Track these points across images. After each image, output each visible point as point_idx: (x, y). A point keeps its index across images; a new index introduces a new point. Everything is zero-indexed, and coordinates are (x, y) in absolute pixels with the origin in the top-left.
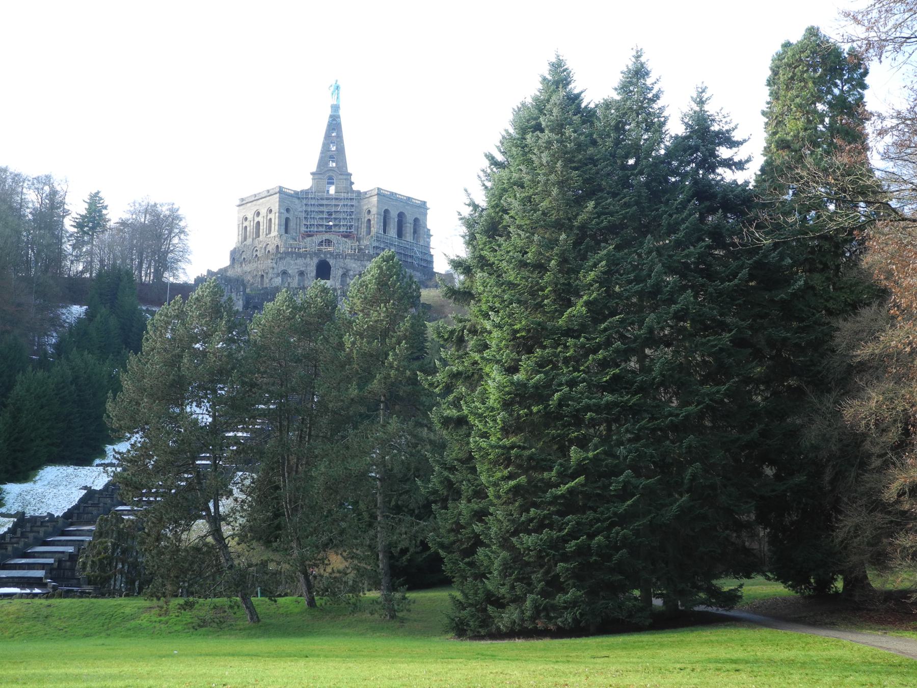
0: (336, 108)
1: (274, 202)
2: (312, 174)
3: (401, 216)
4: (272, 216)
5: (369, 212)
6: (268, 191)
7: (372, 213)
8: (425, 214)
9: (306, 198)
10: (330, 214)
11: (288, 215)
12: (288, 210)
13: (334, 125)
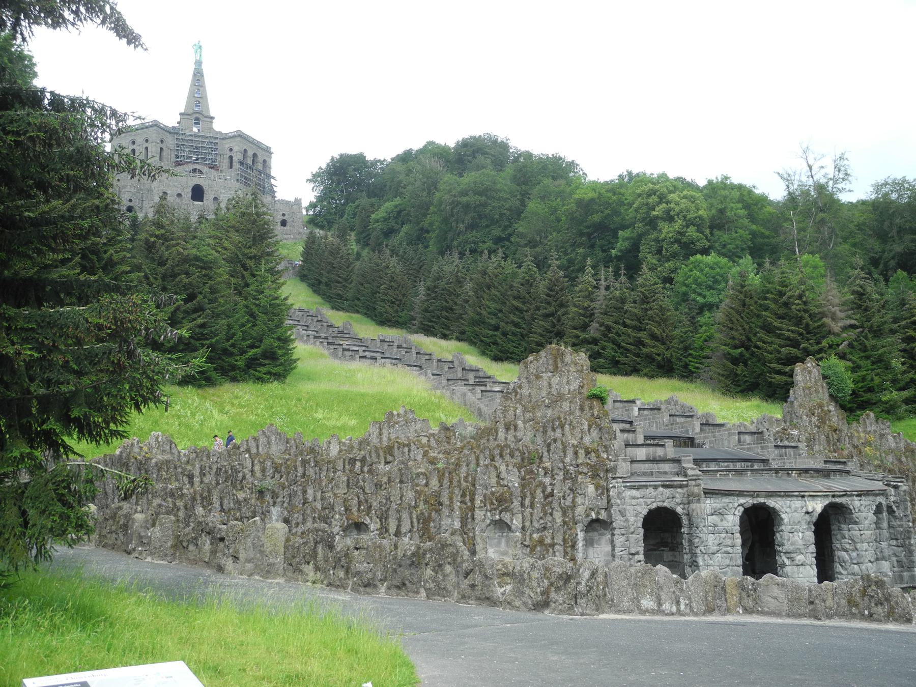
0: (199, 63)
2: (181, 114)
3: (255, 155)
5: (231, 150)
8: (270, 158)
10: (197, 148)
12: (162, 141)
13: (198, 77)
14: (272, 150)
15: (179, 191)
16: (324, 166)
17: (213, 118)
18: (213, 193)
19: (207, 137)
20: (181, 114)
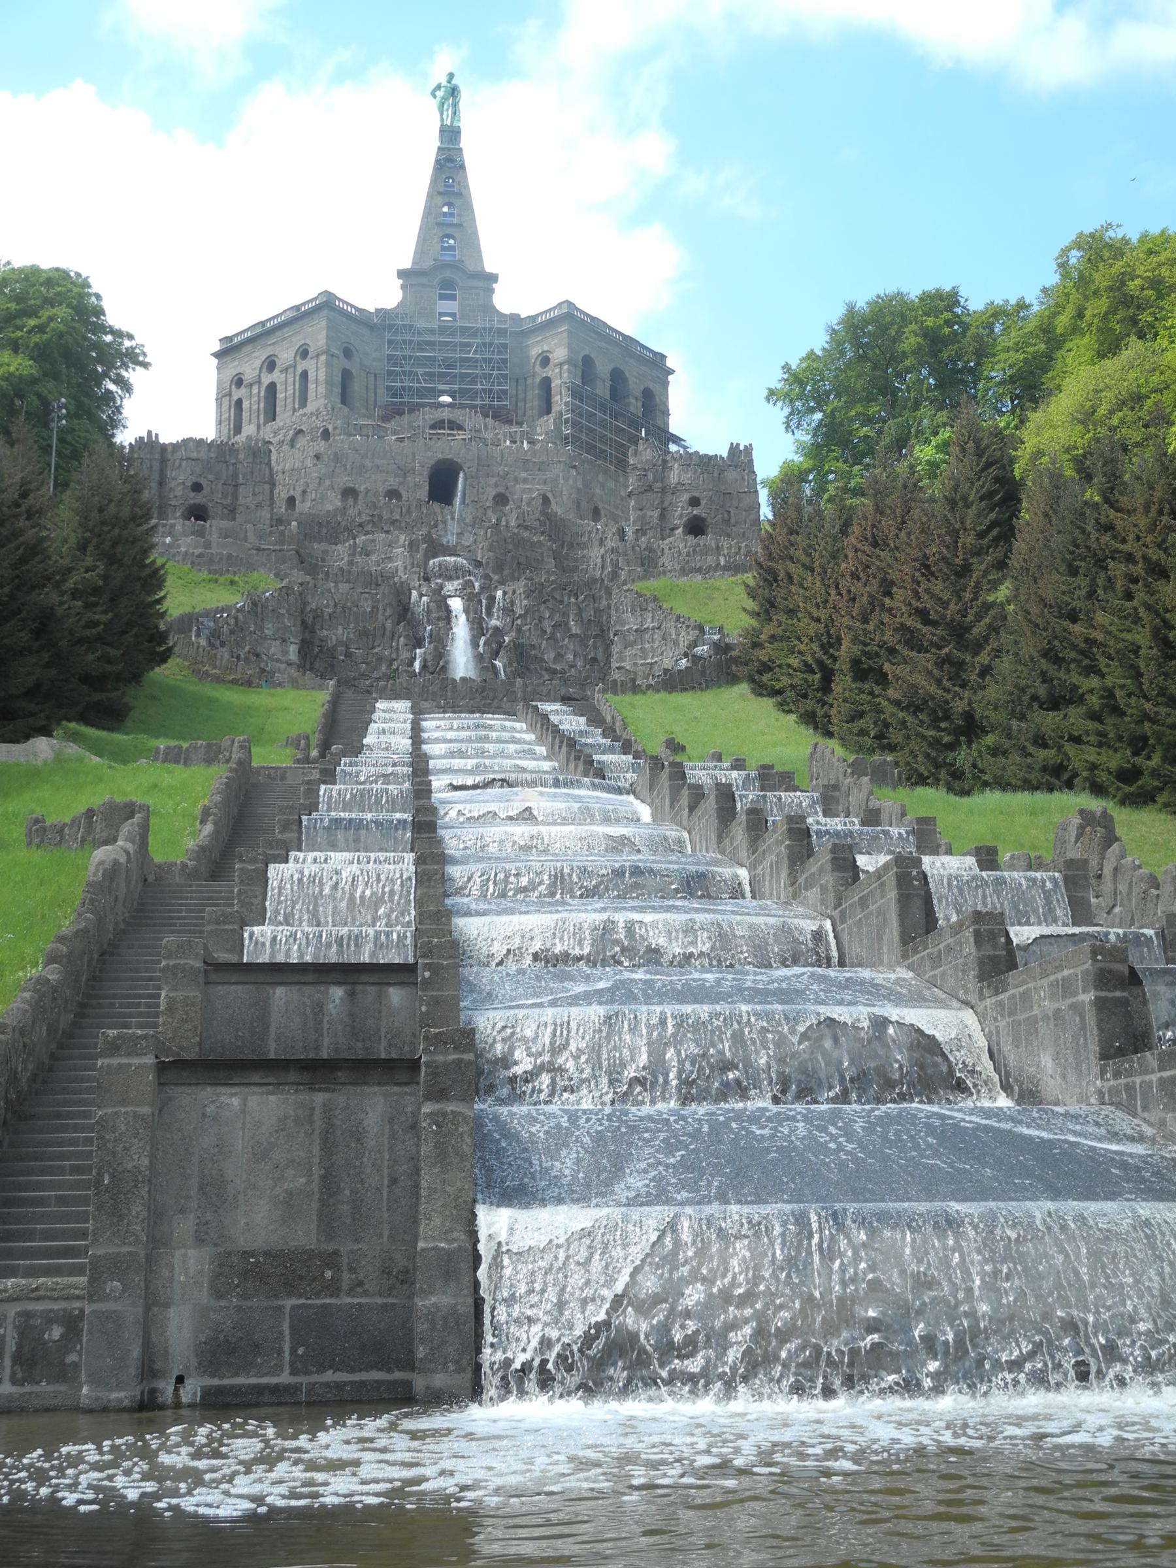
0: (450, 135)
1: (317, 335)
2: (402, 274)
3: (617, 377)
4: (309, 365)
5: (545, 361)
6: (297, 308)
7: (553, 361)
8: (666, 384)
9: (391, 326)
11: (347, 364)
12: (347, 353)
14: (670, 363)
15: (393, 482)
16: (819, 342)
17: (494, 278)
18: (493, 480)
19: (474, 333)
20: (402, 274)
